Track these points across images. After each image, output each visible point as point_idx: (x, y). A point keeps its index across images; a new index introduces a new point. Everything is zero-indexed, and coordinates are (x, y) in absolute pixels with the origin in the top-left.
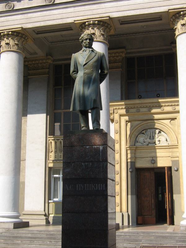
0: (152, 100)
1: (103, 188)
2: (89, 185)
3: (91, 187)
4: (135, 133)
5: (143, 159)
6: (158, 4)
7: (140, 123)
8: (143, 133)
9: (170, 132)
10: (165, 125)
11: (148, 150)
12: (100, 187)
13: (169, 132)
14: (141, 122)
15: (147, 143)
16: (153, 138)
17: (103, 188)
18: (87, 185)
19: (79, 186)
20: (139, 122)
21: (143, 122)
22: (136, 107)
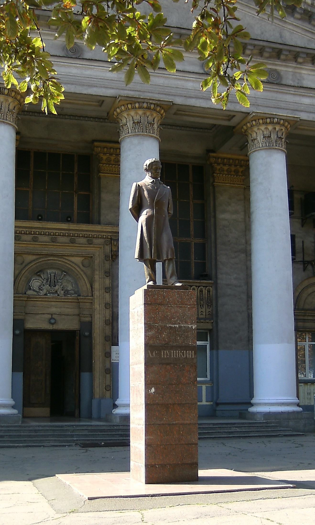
0: (59, 225)
1: (192, 356)
2: (176, 352)
3: (179, 355)
4: (26, 274)
5: (38, 317)
6: (103, 83)
7: (37, 259)
8: (40, 276)
9: (81, 278)
10: (73, 265)
11: (46, 303)
12: (189, 355)
13: (79, 277)
14: (38, 257)
15: (45, 291)
16: (55, 284)
17: (192, 356)
18: (174, 353)
19: (164, 352)
20: (34, 257)
21: (41, 258)
22: (33, 233)
